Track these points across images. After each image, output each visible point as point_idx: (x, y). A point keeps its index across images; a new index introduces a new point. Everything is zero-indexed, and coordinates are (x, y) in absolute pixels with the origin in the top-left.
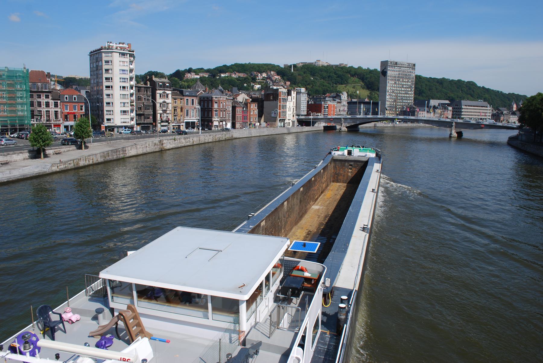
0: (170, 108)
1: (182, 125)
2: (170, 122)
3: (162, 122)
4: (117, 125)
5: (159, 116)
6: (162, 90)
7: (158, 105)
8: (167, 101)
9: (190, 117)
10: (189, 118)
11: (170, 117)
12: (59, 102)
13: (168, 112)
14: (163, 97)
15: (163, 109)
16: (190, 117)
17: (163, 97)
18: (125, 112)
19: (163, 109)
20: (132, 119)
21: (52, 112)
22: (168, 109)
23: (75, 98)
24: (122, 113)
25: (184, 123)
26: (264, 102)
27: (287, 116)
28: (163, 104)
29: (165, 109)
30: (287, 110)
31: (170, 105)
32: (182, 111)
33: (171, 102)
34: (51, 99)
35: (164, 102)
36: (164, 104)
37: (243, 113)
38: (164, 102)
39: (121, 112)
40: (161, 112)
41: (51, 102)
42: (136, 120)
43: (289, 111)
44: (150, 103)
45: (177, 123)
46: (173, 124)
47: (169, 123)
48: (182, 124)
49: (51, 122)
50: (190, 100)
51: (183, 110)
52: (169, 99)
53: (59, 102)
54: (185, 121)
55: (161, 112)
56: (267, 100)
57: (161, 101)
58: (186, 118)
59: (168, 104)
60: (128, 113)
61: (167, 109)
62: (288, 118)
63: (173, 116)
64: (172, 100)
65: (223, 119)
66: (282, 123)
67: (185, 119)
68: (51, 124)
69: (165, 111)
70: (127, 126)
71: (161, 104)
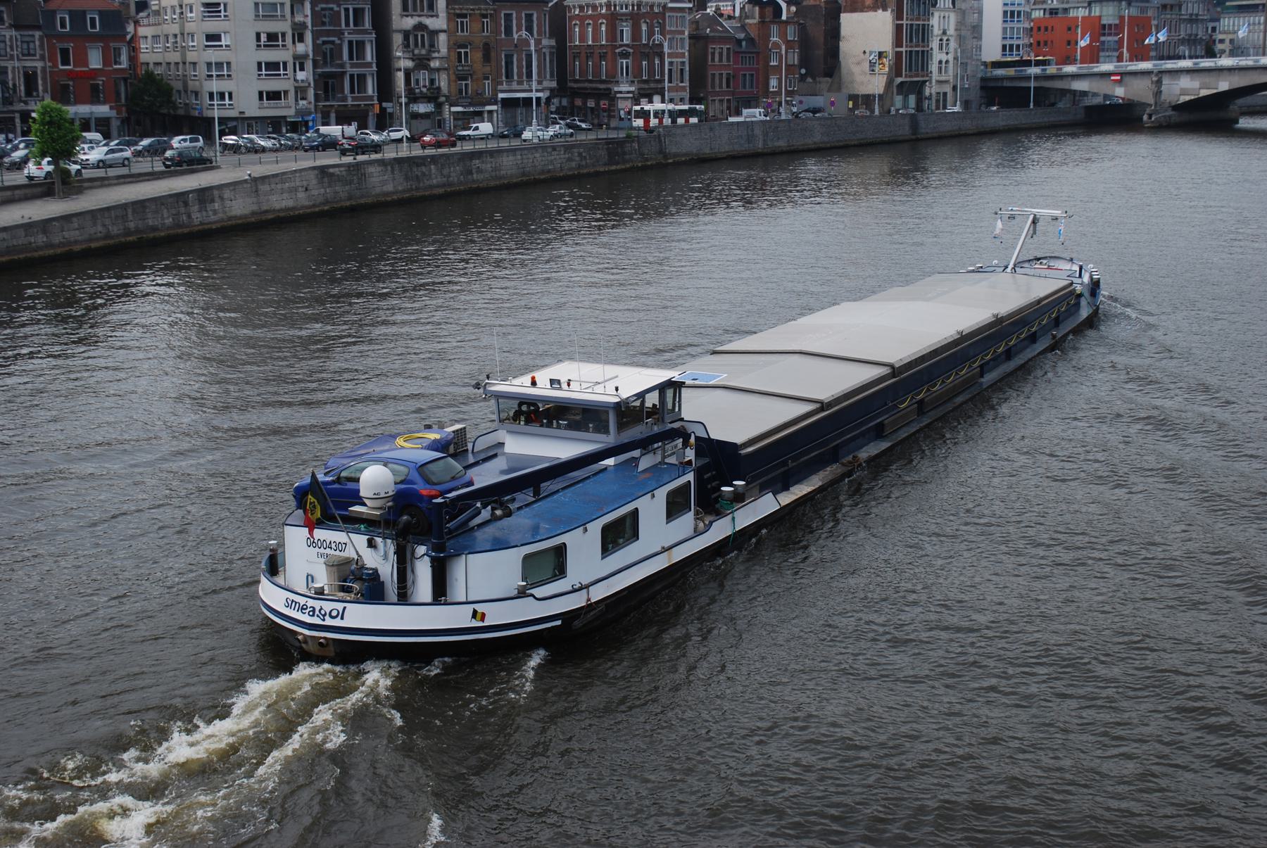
0: (444, 50)
1: (490, 112)
2: (442, 99)
3: (413, 98)
4: (247, 115)
5: (400, 76)
7: (397, 39)
8: (432, 23)
9: (520, 83)
10: (515, 86)
11: (443, 82)
12: (37, 34)
13: (435, 64)
14: (415, 10)
15: (416, 52)
16: (520, 83)
17: (415, 10)
18: (273, 66)
19: (416, 52)
20: (301, 91)
21: (13, 72)
22: (436, 55)
23: (93, 20)
24: (264, 72)
25: (495, 103)
26: (842, 15)
27: (934, 68)
28: (416, 36)
29: (424, 52)
30: (935, 44)
31: (443, 37)
32: (487, 58)
33: (445, 27)
34: (11, 26)
35: (420, 27)
36: (420, 37)
37: (735, 63)
38: (420, 27)
39: (260, 69)
40: (410, 64)
41: (11, 36)
42: (316, 95)
43: (941, 47)
44: (365, 32)
45: (471, 105)
46: (454, 109)
47: (439, 106)
48: (488, 108)
49: (11, 108)
50: (519, 19)
51: (493, 54)
52: (437, 16)
53: (37, 37)
54: (501, 96)
55: (410, 64)
56: (853, 10)
57: (409, 22)
58: (505, 86)
59: (435, 33)
60: (285, 69)
61: (430, 51)
62: (935, 76)
63: (453, 77)
64: (449, 20)
65: (652, 85)
66: (912, 99)
67: (500, 87)
68: (13, 112)
69: (422, 63)
70: (285, 117)
71: (406, 34)
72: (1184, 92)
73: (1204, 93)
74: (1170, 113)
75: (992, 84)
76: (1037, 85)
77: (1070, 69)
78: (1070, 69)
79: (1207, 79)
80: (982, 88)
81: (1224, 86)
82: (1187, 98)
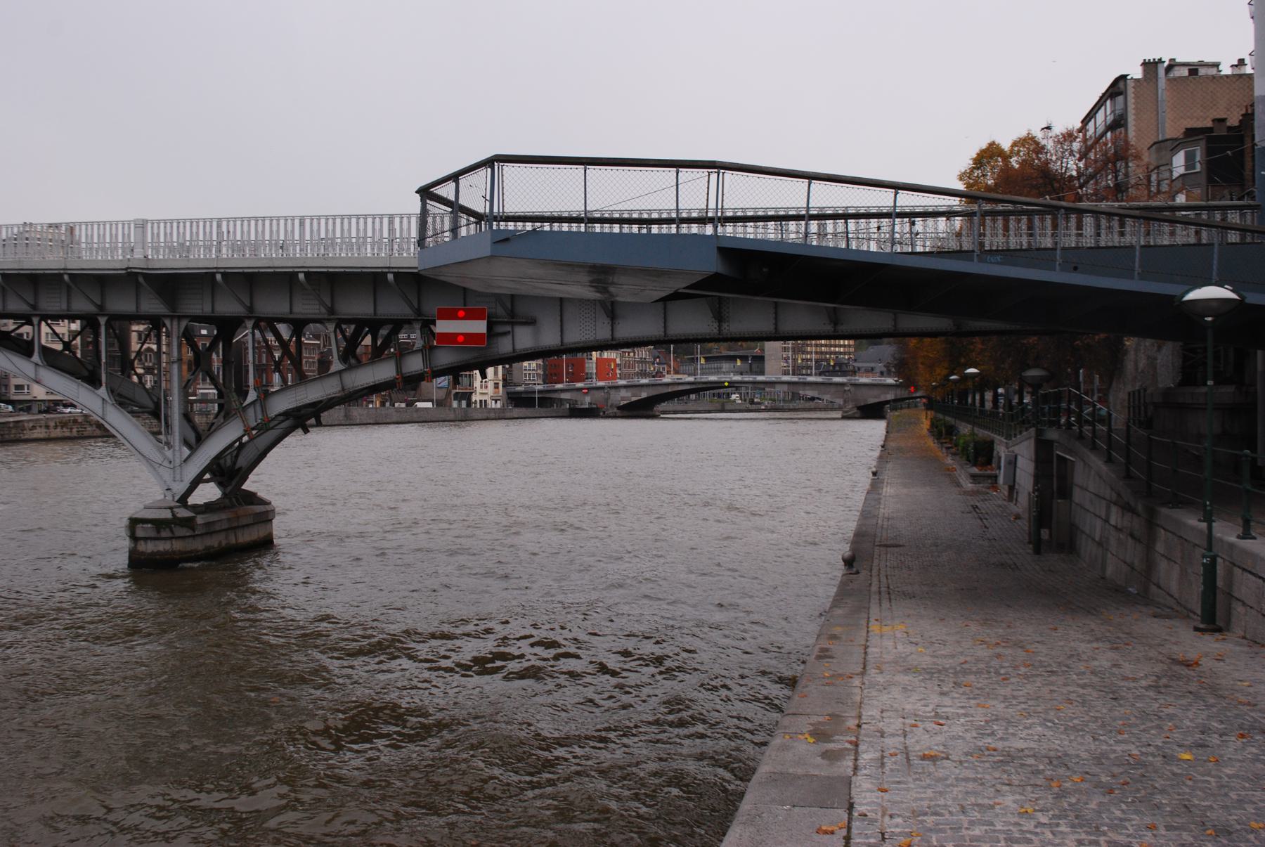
6: (143, 324)
19: (146, 364)
28: (146, 356)
29: (151, 364)
66: (464, 403)
67: (198, 387)
72: (623, 399)
73: (634, 399)
74: (615, 410)
75: (514, 396)
76: (540, 396)
77: (559, 386)
78: (559, 386)
79: (635, 390)
80: (509, 398)
81: (644, 395)
82: (625, 402)
